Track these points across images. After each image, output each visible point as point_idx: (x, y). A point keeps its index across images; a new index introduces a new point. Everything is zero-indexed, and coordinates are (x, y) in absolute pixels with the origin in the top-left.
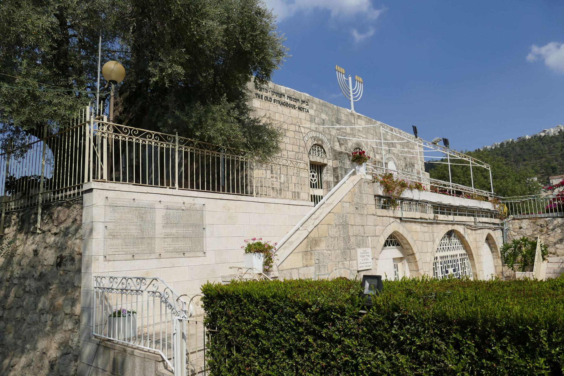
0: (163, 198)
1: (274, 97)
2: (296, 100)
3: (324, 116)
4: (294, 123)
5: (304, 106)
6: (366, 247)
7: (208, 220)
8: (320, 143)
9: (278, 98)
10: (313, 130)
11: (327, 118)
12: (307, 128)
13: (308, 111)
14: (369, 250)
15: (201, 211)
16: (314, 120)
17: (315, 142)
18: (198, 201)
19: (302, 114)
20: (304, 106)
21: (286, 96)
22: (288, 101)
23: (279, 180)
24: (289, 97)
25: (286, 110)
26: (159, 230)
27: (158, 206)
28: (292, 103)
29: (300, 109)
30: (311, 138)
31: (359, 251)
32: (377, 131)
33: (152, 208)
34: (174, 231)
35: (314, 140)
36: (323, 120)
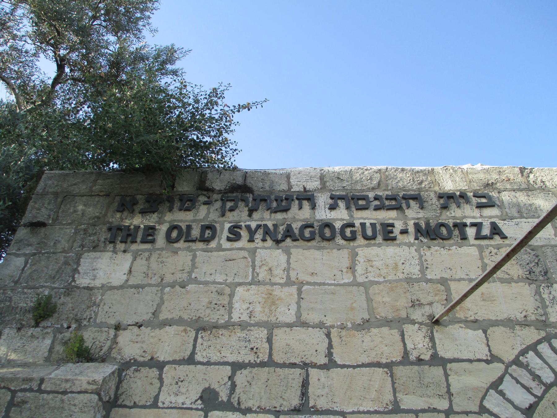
4: (383, 312)
5: (468, 213)
12: (509, 323)
13: (496, 230)
21: (323, 200)
22: (341, 215)
25: (316, 262)
29: (430, 233)
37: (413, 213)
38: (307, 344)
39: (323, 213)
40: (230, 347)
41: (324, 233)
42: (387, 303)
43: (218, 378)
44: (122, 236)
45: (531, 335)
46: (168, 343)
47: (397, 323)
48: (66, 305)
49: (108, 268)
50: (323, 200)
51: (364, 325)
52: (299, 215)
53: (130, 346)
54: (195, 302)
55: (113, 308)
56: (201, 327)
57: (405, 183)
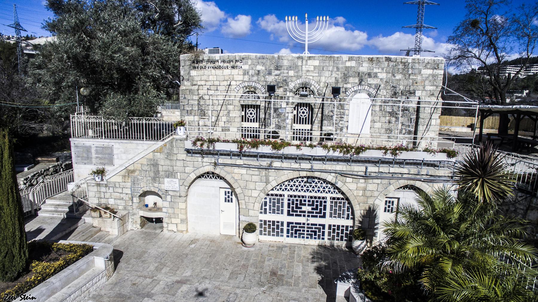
0: (95, 143)
1: (209, 65)
2: (229, 62)
3: (259, 67)
6: (175, 178)
7: (115, 152)
8: (252, 89)
9: (212, 65)
10: (245, 81)
11: (264, 68)
14: (177, 180)
15: (111, 148)
16: (248, 73)
17: (248, 90)
18: (110, 144)
19: (235, 71)
20: (238, 64)
21: (220, 61)
23: (210, 120)
24: (224, 61)
25: (218, 72)
26: (94, 155)
27: (92, 146)
28: (226, 65)
29: (233, 67)
30: (243, 87)
31: (166, 180)
32: (340, 66)
33: (90, 147)
34: (100, 156)
35: (246, 88)
36: (259, 71)
37: (232, 63)
38: (217, 83)
39: (220, 64)
40: (209, 83)
41: (219, 68)
42: (227, 78)
43: (209, 87)
44: (194, 68)
45: (241, 82)
46: (203, 83)
47: (227, 80)
48: (190, 78)
49: (193, 73)
50: (220, 61)
51: (224, 81)
52: (217, 64)
53: (199, 83)
54: (204, 78)
55: (196, 78)
56: (206, 81)
57: (232, 58)
